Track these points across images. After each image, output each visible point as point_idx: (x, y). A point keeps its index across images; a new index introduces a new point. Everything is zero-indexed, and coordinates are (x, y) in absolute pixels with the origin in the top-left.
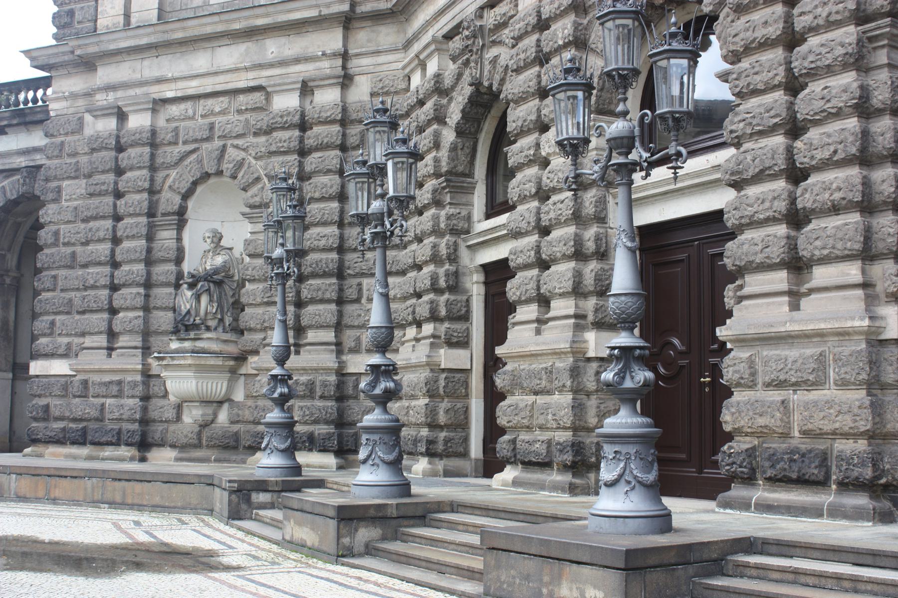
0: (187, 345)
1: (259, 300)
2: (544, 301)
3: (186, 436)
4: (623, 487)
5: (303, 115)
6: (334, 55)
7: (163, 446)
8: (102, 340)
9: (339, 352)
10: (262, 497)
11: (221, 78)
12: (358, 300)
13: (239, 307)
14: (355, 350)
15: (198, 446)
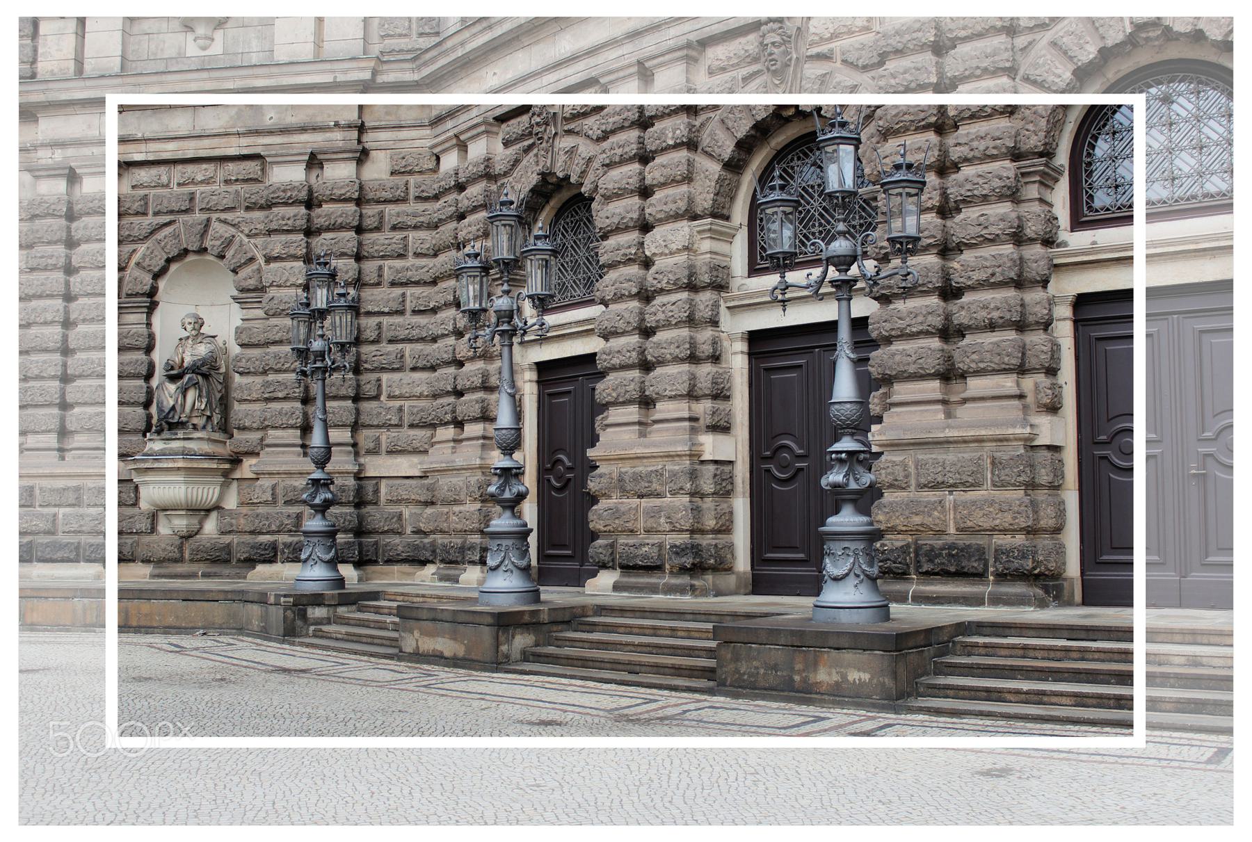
0: (175, 445)
1: (255, 396)
2: (646, 402)
3: (164, 550)
4: (852, 581)
5: (310, 191)
6: (350, 126)
7: (134, 561)
8: (52, 440)
9: (357, 454)
10: (317, 612)
11: (206, 142)
12: (376, 398)
13: (225, 404)
14: (374, 452)
15: (180, 560)
